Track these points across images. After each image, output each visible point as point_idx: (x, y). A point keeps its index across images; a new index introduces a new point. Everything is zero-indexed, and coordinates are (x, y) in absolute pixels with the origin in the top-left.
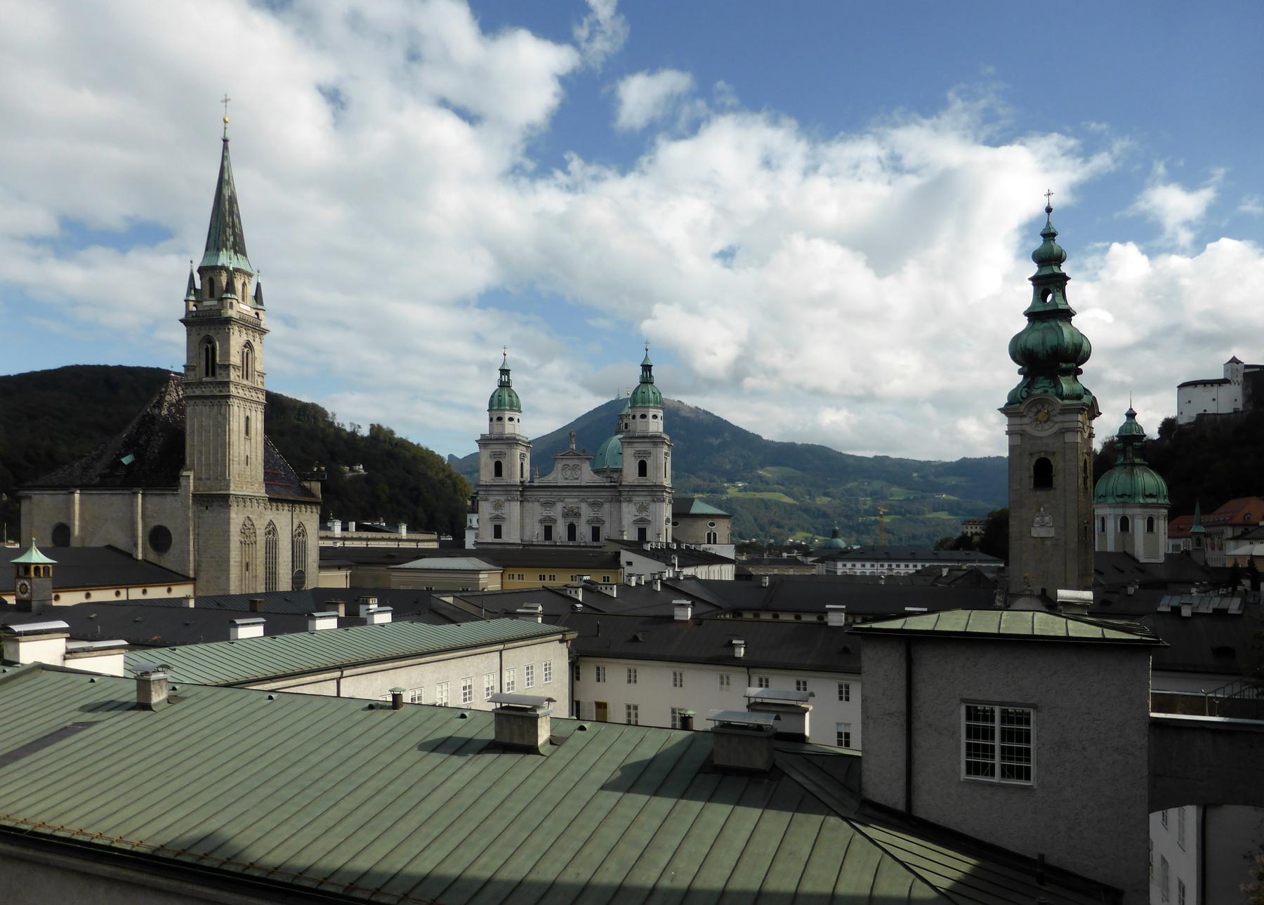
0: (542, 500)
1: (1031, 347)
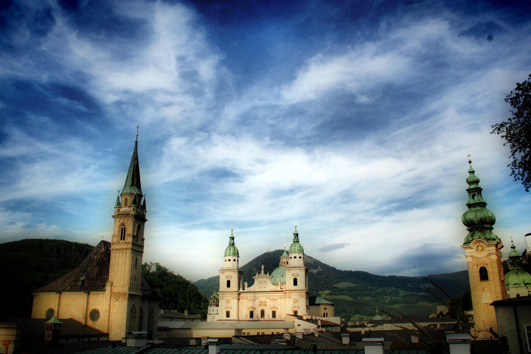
0: (249, 298)
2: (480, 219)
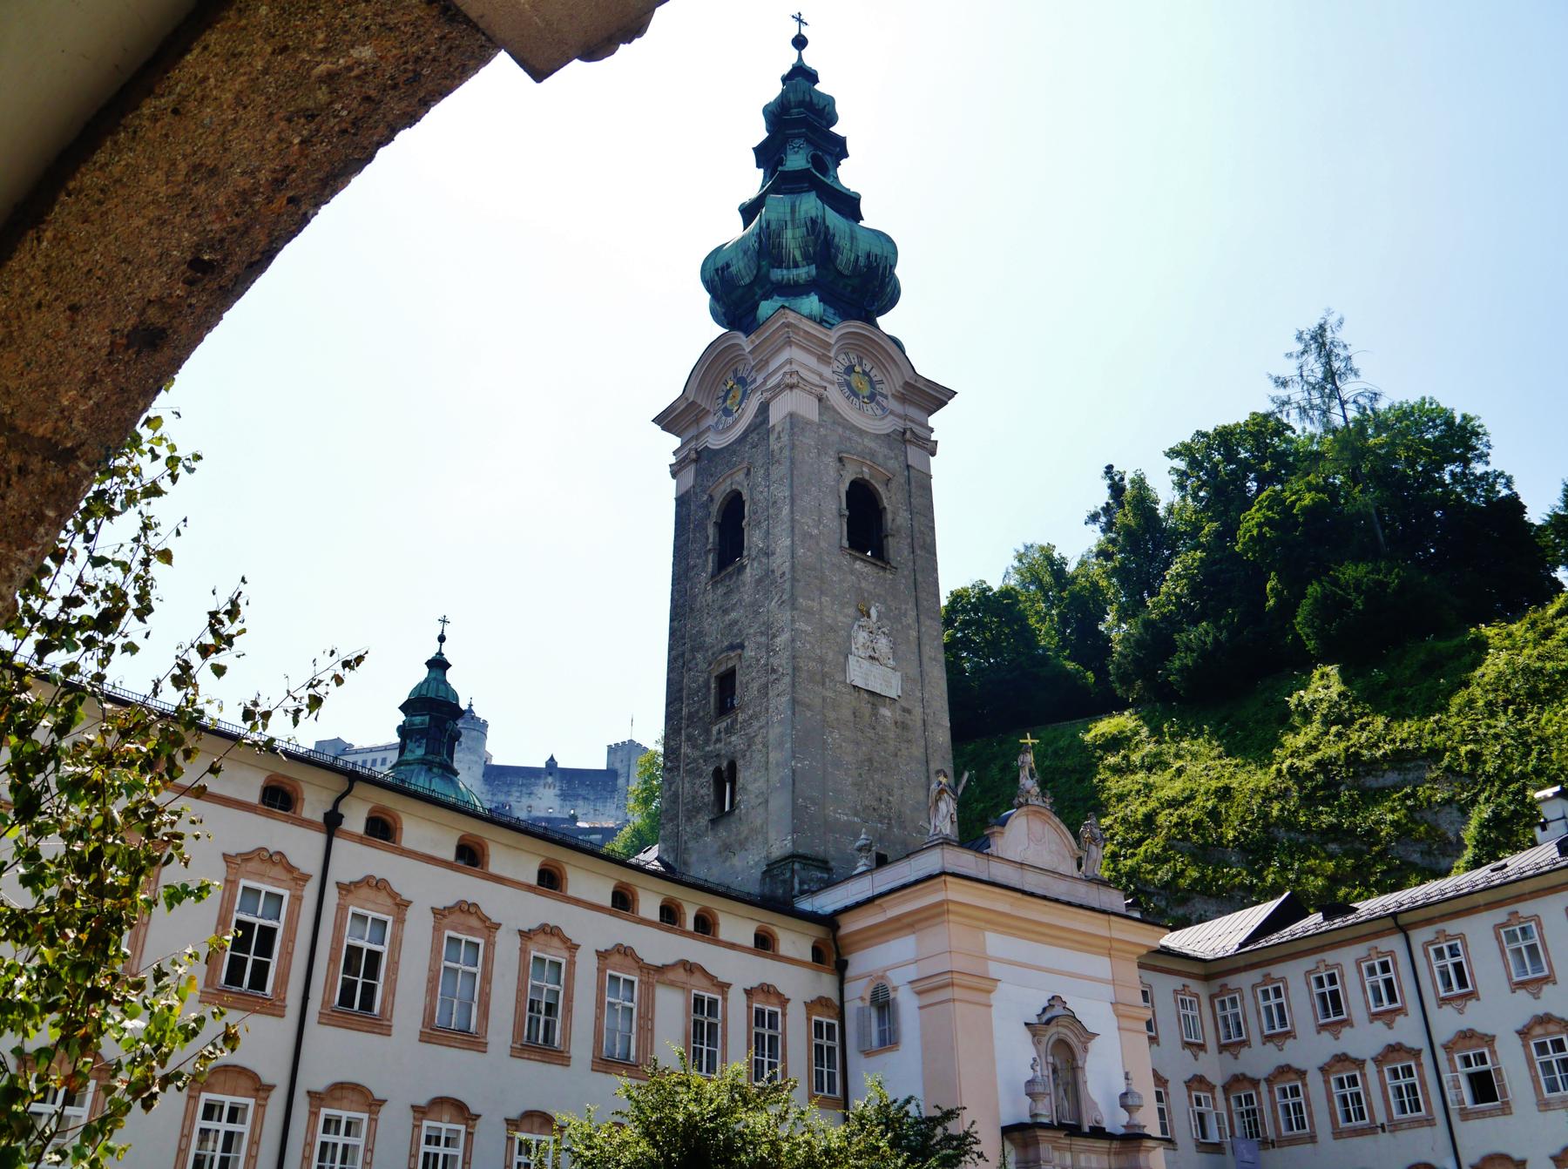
1: (831, 227)
2: (868, 255)
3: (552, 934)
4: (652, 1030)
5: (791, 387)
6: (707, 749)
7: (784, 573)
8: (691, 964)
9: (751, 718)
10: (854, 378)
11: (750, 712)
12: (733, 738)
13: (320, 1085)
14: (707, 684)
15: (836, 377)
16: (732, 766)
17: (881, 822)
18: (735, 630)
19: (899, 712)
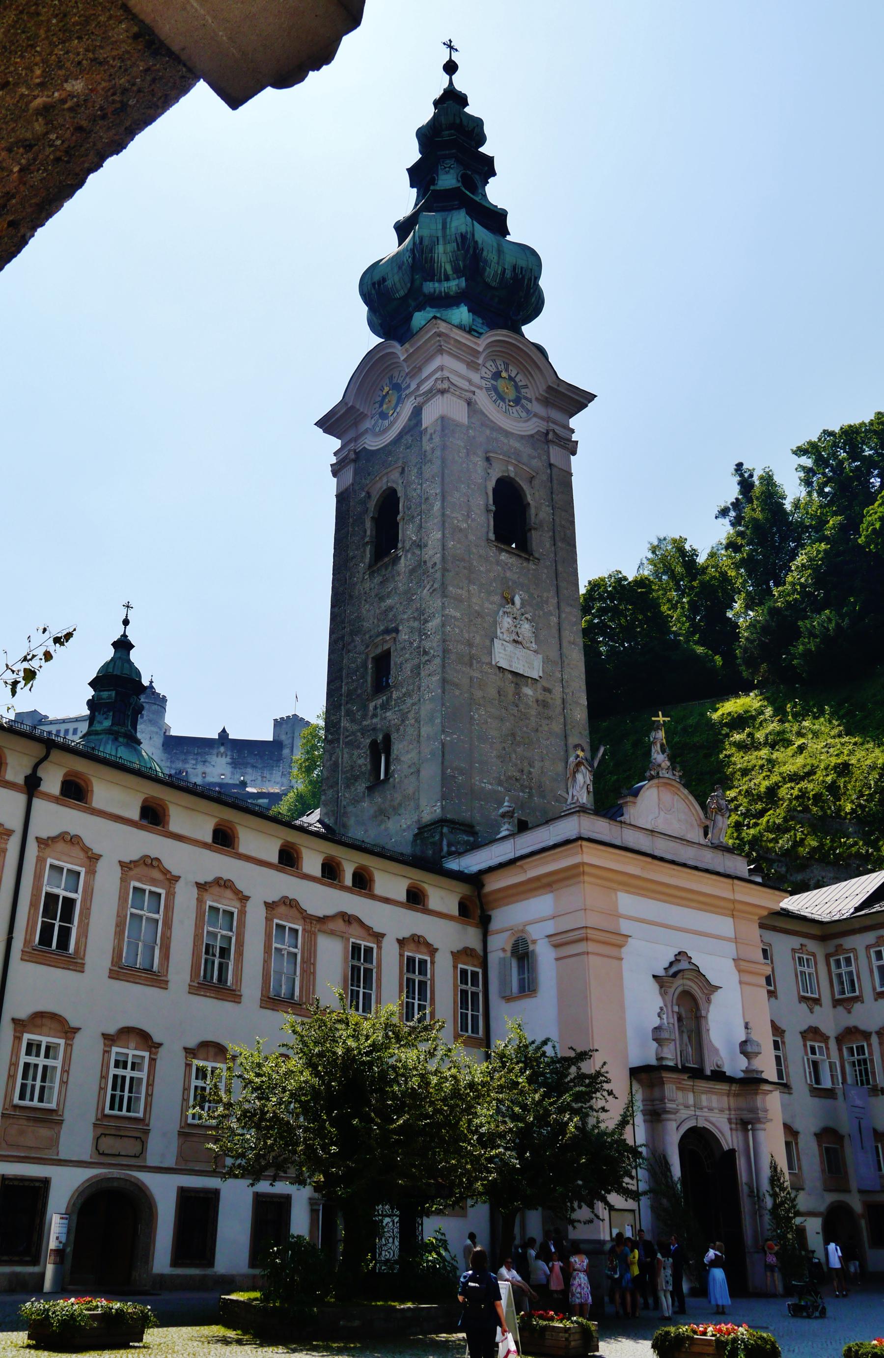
1: (480, 242)
3: (225, 886)
4: (314, 973)
5: (443, 392)
6: (365, 723)
7: (435, 564)
8: (349, 916)
9: (404, 695)
10: (501, 384)
11: (404, 690)
12: (388, 714)
13: (23, 1013)
14: (364, 665)
15: (483, 383)
16: (387, 739)
17: (523, 792)
18: (391, 615)
19: (540, 691)
